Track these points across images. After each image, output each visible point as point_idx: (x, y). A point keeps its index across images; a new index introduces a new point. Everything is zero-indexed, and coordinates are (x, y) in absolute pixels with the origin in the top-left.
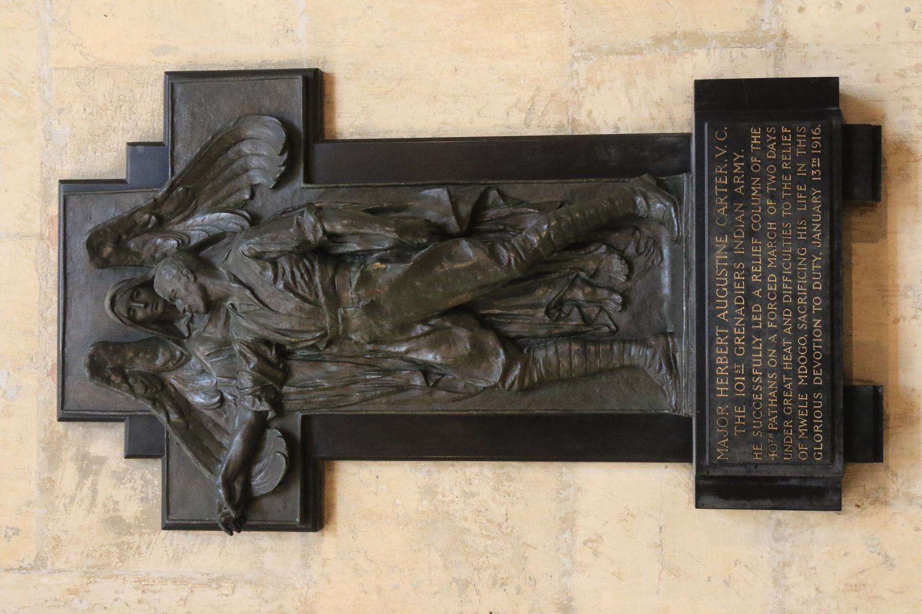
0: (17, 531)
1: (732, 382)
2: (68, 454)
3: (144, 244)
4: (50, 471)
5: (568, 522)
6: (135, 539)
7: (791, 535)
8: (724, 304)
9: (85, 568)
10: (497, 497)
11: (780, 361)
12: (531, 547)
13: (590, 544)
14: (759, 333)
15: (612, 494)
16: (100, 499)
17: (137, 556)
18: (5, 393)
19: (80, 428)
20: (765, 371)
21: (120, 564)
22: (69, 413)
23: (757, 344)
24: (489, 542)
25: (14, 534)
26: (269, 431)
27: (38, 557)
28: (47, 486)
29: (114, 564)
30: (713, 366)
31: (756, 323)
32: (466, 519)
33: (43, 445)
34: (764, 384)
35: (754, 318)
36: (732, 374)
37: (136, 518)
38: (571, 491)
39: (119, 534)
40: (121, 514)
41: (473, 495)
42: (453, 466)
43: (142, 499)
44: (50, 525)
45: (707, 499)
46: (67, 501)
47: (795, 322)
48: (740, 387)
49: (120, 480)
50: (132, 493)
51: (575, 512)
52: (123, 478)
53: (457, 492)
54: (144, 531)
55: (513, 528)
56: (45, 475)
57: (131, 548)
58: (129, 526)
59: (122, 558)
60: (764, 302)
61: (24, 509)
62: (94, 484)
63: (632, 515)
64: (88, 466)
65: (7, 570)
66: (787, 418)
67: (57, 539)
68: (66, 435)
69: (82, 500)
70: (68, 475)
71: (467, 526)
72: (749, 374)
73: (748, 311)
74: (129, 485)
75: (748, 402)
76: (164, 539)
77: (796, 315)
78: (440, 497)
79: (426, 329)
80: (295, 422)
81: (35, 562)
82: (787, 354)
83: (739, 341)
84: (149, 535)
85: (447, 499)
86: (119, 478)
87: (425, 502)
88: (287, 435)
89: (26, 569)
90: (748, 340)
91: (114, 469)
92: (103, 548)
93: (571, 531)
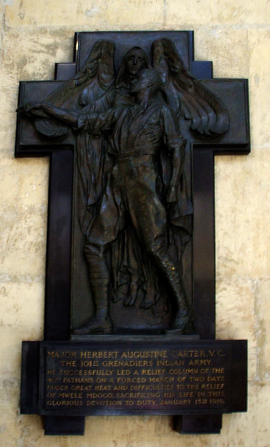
0: (22, 18)
1: (89, 360)
2: (58, 40)
3: (163, 67)
4: (50, 32)
5: (15, 279)
6: (15, 71)
7: (6, 389)
8: (130, 355)
9: (2, 49)
10: (28, 244)
11: (100, 384)
12: (3, 261)
13: (3, 290)
14: (115, 373)
15: (28, 301)
16: (35, 55)
17: (7, 72)
18: (89, 11)
19: (70, 45)
20: (95, 376)
21: (4, 64)
22: (78, 37)
23: (108, 372)
24: (5, 240)
25: (21, 17)
26: (66, 128)
27: (9, 28)
28: (43, 31)
29: (4, 62)
30: (97, 350)
31: (120, 372)
32: (17, 228)
33: (63, 28)
34: (87, 376)
35: (123, 371)
36: (93, 360)
37: (25, 71)
38: (30, 281)
39: (18, 64)
40: (28, 64)
41: (29, 232)
42: (44, 222)
43: (34, 74)
44: (24, 33)
45: (27, 347)
46: (35, 40)
47: (120, 392)
48: (86, 363)
49: (44, 63)
50: (38, 69)
51: (19, 283)
52: (45, 65)
53: (31, 224)
54: (19, 75)
55: (12, 252)
56: (48, 30)
57: (11, 70)
58: (22, 68)
59: (6, 66)
60: (131, 376)
61: (33, 21)
62: (42, 52)
63: (17, 311)
64: (52, 49)
65: (4, 15)
66: (70, 387)
67: (17, 36)
68: (67, 38)
69: (35, 47)
70: (48, 40)
71: (14, 229)
72: (93, 368)
73: (126, 368)
74: (41, 67)
75: (78, 368)
76: (14, 84)
77: (124, 392)
78: (28, 216)
79: (119, 204)
80: (71, 140)
81: (7, 27)
82: (103, 387)
83: (110, 363)
84: (17, 77)
85: (27, 219)
86: (45, 63)
87: (26, 208)
88: (65, 136)
89: (4, 23)
90: (111, 368)
91: (50, 60)
92: (11, 57)
93: (10, 281)
